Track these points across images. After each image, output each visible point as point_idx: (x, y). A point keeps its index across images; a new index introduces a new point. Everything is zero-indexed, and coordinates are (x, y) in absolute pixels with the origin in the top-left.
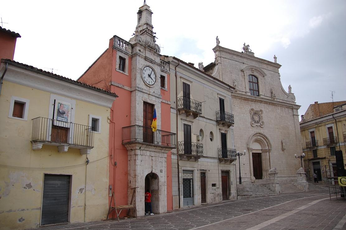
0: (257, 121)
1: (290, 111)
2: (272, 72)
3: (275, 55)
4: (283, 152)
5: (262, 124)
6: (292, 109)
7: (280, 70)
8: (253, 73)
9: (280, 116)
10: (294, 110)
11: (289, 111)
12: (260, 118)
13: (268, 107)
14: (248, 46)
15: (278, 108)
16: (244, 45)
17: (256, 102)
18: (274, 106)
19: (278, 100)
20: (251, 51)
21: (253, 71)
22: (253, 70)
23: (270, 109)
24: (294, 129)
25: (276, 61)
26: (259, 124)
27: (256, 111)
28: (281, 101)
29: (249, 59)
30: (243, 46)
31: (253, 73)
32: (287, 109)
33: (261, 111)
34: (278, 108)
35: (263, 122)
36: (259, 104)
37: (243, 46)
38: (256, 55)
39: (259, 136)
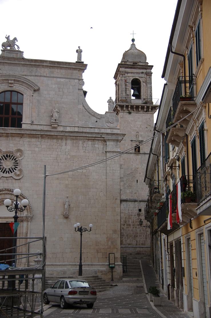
0: (7, 170)
1: (99, 145)
2: (62, 80)
3: (79, 47)
4: (65, 221)
5: (18, 173)
6: (105, 141)
7: (86, 75)
8: (10, 87)
9: (69, 157)
10: (108, 143)
11: (96, 146)
12: (16, 163)
13: (39, 143)
14: (15, 39)
15: (66, 144)
16: (8, 38)
17: (10, 138)
18: (55, 141)
19: (68, 129)
20: (18, 48)
21: (11, 83)
22: (10, 82)
23: (45, 146)
24: (104, 177)
25: (79, 57)
26: (13, 173)
27: (6, 152)
28: (76, 129)
29: (6, 63)
30: (5, 40)
31: (10, 87)
32: (90, 143)
33: (19, 150)
34: (66, 144)
35: (20, 170)
36: (17, 139)
37: (5, 40)
38: (26, 56)
39: (6, 194)
